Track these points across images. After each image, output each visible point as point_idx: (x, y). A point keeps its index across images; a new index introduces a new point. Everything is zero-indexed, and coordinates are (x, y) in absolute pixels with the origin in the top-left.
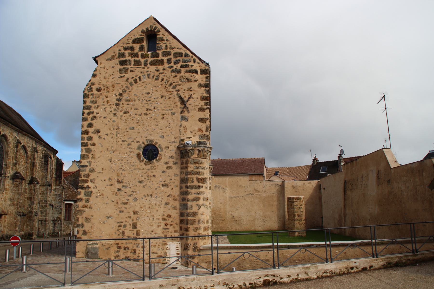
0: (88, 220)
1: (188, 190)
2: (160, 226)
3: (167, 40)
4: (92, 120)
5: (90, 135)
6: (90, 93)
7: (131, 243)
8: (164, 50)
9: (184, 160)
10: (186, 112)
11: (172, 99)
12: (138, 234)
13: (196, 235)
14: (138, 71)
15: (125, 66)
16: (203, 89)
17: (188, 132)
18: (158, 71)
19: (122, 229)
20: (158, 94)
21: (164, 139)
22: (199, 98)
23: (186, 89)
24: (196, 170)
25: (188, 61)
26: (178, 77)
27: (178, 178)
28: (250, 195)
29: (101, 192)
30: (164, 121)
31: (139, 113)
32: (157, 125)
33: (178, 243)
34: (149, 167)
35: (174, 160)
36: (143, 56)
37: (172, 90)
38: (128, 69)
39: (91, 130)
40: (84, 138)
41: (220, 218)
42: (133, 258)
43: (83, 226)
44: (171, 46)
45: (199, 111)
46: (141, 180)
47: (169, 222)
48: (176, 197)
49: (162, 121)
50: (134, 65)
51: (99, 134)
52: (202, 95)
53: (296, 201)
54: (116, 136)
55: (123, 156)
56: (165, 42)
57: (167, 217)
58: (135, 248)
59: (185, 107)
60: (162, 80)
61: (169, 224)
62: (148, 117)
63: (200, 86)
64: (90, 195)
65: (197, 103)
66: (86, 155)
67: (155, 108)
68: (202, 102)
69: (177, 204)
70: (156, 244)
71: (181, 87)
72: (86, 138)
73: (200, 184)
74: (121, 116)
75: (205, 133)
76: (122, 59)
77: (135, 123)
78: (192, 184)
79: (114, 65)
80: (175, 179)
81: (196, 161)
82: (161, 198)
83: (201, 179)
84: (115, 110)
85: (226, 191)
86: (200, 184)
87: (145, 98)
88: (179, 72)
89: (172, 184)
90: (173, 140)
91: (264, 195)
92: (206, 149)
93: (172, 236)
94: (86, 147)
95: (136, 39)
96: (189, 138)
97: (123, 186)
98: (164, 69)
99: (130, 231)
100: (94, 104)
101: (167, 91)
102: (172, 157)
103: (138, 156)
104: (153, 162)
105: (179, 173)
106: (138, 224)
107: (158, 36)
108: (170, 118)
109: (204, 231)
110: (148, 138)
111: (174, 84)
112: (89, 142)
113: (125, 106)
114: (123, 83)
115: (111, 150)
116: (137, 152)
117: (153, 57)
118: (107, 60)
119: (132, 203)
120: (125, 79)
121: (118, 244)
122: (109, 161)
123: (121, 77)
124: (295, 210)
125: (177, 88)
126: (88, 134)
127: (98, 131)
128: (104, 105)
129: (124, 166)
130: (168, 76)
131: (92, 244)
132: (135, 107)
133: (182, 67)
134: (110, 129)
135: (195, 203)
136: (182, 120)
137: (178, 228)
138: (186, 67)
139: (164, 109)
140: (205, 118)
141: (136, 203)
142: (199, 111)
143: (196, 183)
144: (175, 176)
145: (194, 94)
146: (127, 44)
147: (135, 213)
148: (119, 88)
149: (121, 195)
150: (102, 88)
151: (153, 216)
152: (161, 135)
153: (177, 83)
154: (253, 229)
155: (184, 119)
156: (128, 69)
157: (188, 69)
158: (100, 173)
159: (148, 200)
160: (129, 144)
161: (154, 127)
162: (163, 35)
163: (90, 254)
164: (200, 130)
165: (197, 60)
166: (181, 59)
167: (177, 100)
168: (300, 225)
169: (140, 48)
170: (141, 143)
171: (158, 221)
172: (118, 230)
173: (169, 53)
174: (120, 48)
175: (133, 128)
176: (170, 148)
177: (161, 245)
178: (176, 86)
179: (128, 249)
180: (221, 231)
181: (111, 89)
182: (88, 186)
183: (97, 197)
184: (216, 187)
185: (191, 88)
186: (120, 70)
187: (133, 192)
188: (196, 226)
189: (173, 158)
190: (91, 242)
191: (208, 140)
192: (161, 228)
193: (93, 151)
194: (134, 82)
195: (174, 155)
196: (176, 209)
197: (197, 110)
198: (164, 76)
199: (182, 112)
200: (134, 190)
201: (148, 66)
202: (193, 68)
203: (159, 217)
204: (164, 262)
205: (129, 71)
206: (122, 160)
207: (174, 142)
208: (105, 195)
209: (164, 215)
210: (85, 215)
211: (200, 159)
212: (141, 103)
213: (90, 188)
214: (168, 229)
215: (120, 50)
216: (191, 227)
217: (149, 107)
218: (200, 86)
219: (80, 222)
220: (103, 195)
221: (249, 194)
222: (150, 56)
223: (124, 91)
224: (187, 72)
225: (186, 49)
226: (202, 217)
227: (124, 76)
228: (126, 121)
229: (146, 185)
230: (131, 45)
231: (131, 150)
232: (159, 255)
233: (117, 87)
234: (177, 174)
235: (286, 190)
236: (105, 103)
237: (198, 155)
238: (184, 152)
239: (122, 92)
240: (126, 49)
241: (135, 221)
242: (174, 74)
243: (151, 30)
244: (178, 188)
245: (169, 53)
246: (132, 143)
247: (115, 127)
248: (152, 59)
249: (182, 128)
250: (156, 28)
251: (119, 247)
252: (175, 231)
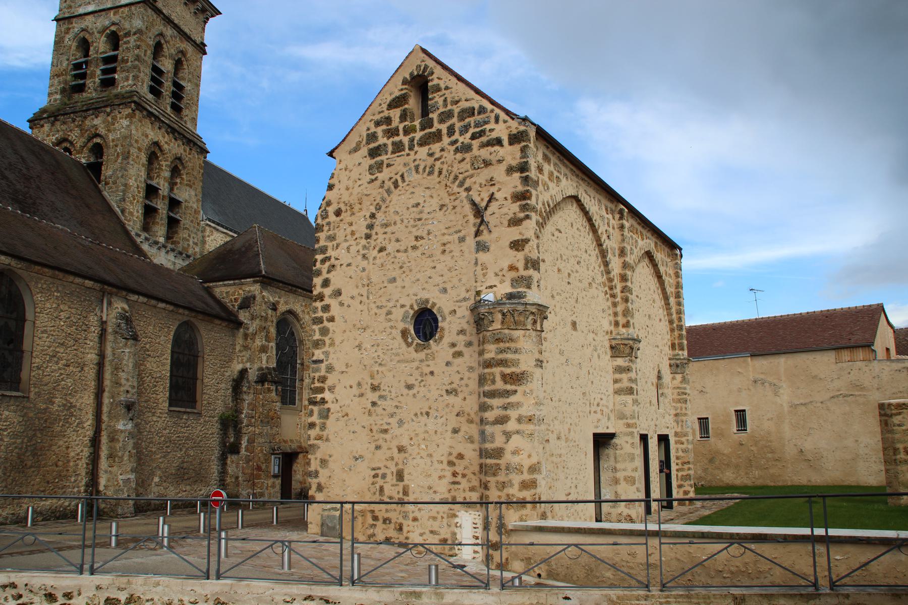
0: (324, 462)
1: (486, 399)
2: (444, 476)
3: (447, 88)
4: (329, 272)
5: (327, 301)
6: (324, 223)
7: (395, 510)
8: (442, 110)
9: (481, 335)
10: (485, 232)
11: (458, 209)
12: (406, 493)
13: (503, 500)
14: (399, 163)
15: (378, 159)
16: (517, 175)
17: (491, 274)
18: (431, 155)
19: (380, 482)
20: (435, 203)
21: (447, 296)
22: (509, 198)
23: (484, 183)
24: (501, 356)
25: (486, 123)
26: (468, 160)
27: (475, 376)
28: (841, 398)
29: (345, 410)
30: (447, 257)
31: (402, 248)
32: (435, 267)
33: (477, 513)
34: (422, 355)
35: (467, 338)
36: (407, 131)
37: (458, 190)
38: (382, 162)
39: (327, 291)
40: (317, 308)
41: (770, 455)
42: (397, 541)
43: (316, 474)
44: (453, 98)
45: (509, 226)
46: (410, 383)
47: (459, 469)
48: (473, 415)
49: (443, 258)
50: (393, 153)
51: (340, 298)
52: (514, 190)
53: (900, 414)
54: (368, 298)
55: (380, 337)
56: (443, 92)
57: (457, 458)
58: (401, 520)
59: (482, 221)
60: (440, 173)
61: (460, 473)
62: (418, 253)
63: (510, 170)
64: (327, 417)
65: (504, 210)
66: (321, 340)
67: (429, 234)
68: (514, 205)
69: (474, 430)
70: (436, 515)
71: (473, 180)
72: (320, 309)
73: (509, 387)
74: (375, 258)
75: (522, 272)
76: (372, 145)
77: (397, 269)
78: (492, 387)
79: (361, 160)
80: (469, 378)
81: (499, 336)
82: (444, 419)
83: (511, 375)
84: (365, 247)
85: (781, 391)
86: (509, 387)
87: (412, 216)
88: (467, 148)
89: (464, 388)
90: (464, 294)
92: (521, 308)
93: (465, 498)
94: (321, 326)
95: (393, 100)
96: (491, 287)
97: (381, 397)
98: (442, 150)
99: (392, 485)
100: (331, 241)
101: (449, 195)
102: (462, 332)
103: (404, 333)
104: (429, 344)
105: (475, 365)
106: (406, 473)
107: (430, 84)
108: (455, 247)
109: (520, 490)
110: (418, 297)
111: (461, 177)
112: (325, 315)
113: (381, 237)
114: (375, 192)
115: (359, 326)
116: (401, 326)
117: (422, 129)
118: (350, 152)
119: (395, 430)
120: (378, 183)
121: (372, 511)
122: (357, 349)
123: (372, 181)
125: (466, 185)
126: (322, 300)
127: (338, 293)
128: (346, 241)
129: (382, 355)
130: (449, 162)
131: (329, 510)
132: (397, 235)
133: (473, 137)
134: (357, 287)
135: (498, 428)
136: (477, 251)
137: (476, 483)
138: (481, 136)
139: (446, 231)
140: (522, 240)
141: (401, 430)
142: (509, 226)
143: (500, 385)
144: (468, 371)
145: (499, 190)
146: (380, 113)
147: (401, 449)
148: (369, 203)
149: (377, 415)
150: (343, 208)
151: (431, 456)
152: (441, 286)
153: (467, 174)
154: (851, 481)
155: (482, 247)
156: (382, 162)
157: (484, 139)
158: (343, 372)
159: (422, 424)
160: (389, 313)
161: (428, 273)
162: (439, 78)
163: (331, 530)
164: (512, 268)
165: (503, 116)
166: (471, 120)
167: (468, 209)
169: (401, 117)
170: (407, 308)
171: (440, 466)
172: (373, 484)
173: (450, 114)
174: (369, 124)
175: (394, 280)
176: (459, 313)
177: (445, 516)
178: (465, 179)
179: (390, 522)
180: (772, 484)
181: (357, 207)
182: (323, 399)
183: (338, 420)
184: (755, 382)
185: (491, 180)
186: (371, 168)
187: (397, 407)
188: (501, 478)
189: (465, 334)
190: (329, 506)
191: (529, 287)
192: (445, 481)
193: (331, 331)
194: (392, 187)
195: (466, 326)
196: (472, 442)
197: (506, 223)
198: (443, 163)
199: (478, 233)
200: (398, 404)
201: (416, 148)
202: (494, 135)
203: (443, 458)
204: (451, 553)
205: (385, 166)
206: (378, 346)
207: (465, 299)
208: (350, 416)
209: (450, 454)
210: (319, 454)
211: (507, 331)
212: (407, 227)
213: (327, 402)
214: (458, 483)
215: (368, 129)
216: (492, 480)
217: (419, 234)
218: (510, 170)
219: (312, 468)
220: (347, 415)
221: (837, 396)
222: (418, 127)
223: (378, 208)
224: (483, 146)
225: (480, 98)
226: (515, 460)
227: (376, 179)
228: (382, 265)
229: (418, 392)
230: (386, 113)
231: (392, 324)
232: (442, 537)
233: (366, 202)
234: (471, 368)
236: (349, 237)
237: (502, 323)
238: (480, 318)
239: (374, 211)
240: (378, 124)
241: (400, 467)
242: (459, 156)
243: (418, 75)
244: (475, 397)
245: (450, 114)
246: (394, 310)
247: (365, 282)
248: (423, 133)
249: (479, 268)
250: (426, 67)
251: (375, 518)
252: (472, 489)
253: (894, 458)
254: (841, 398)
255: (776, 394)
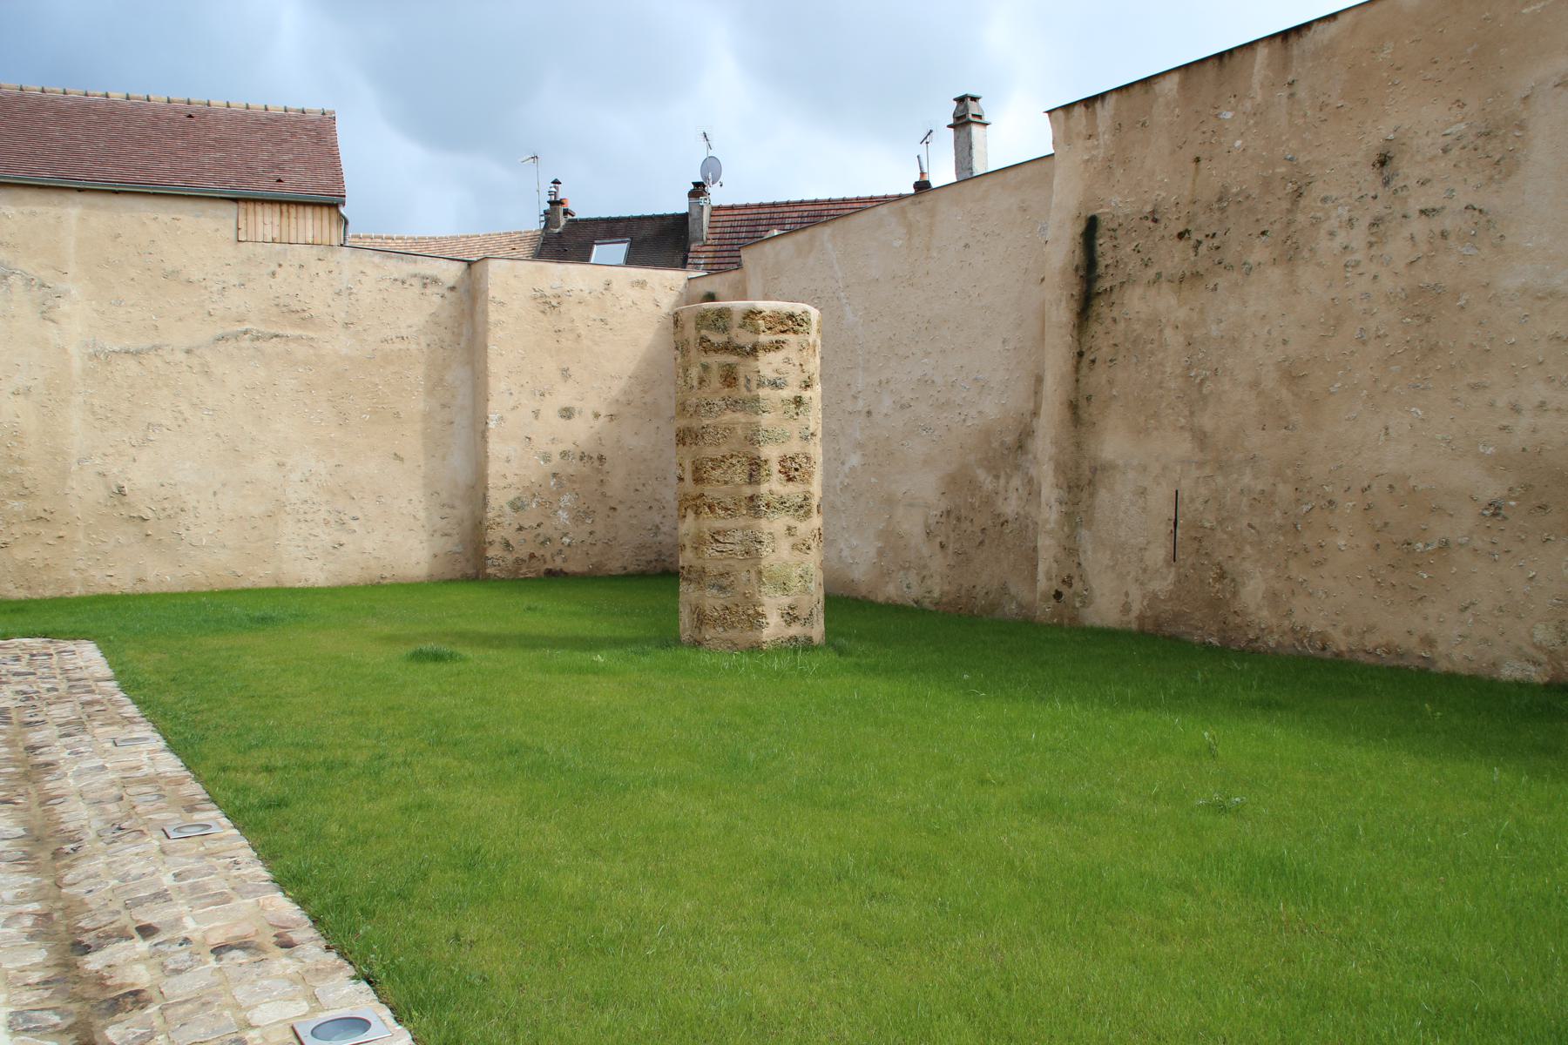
28: (245, 342)
41: (17, 505)
53: (777, 346)
85: (65, 306)
91: (340, 344)
124: (766, 420)
154: (260, 575)
168: (803, 547)
180: (21, 594)
221: (236, 337)
235: (494, 315)
253: (748, 491)
254: (245, 342)
255: (46, 314)
